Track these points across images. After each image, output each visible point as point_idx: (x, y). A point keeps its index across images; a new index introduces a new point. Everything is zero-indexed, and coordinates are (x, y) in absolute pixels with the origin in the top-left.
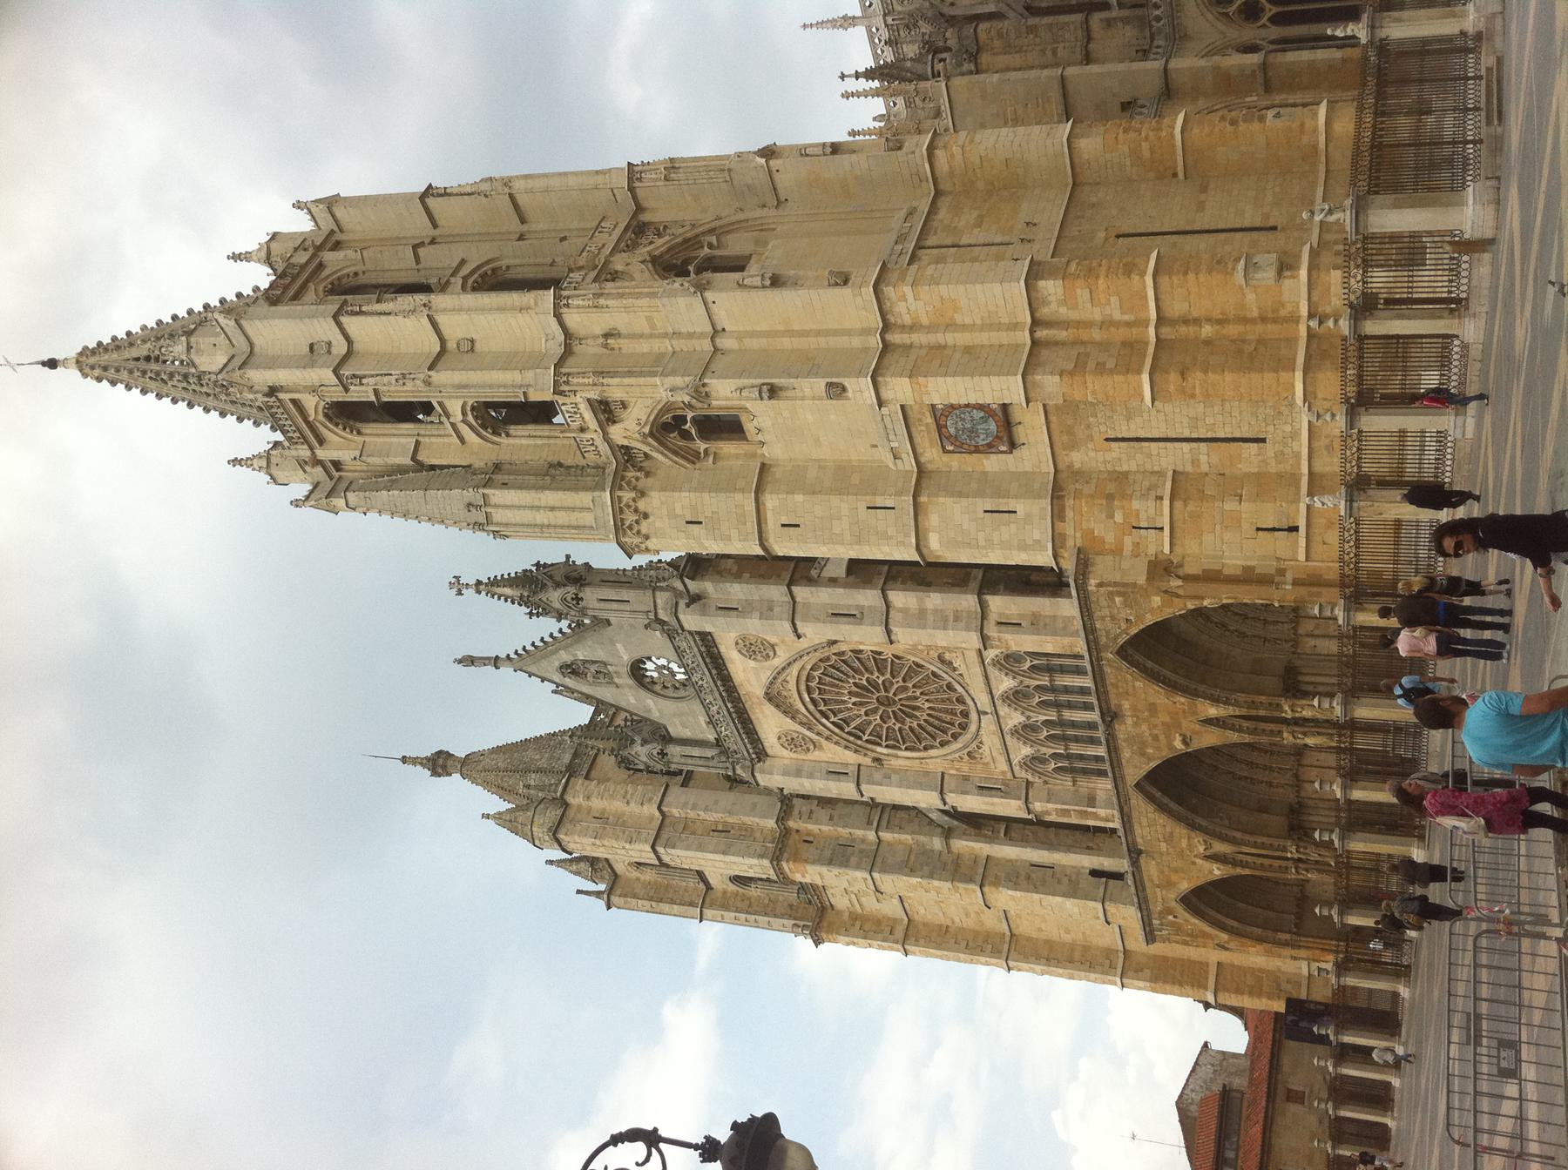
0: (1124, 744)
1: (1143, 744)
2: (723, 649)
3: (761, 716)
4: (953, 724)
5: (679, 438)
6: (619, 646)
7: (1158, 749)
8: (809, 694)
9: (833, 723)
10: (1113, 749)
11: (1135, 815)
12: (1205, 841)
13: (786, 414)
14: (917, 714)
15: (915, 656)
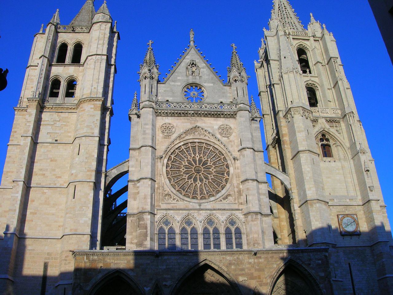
0: (235, 257)
1: (238, 264)
2: (221, 119)
3: (183, 121)
4: (186, 192)
5: (321, 138)
6: (212, 85)
7: (235, 270)
8: (198, 142)
9: (180, 146)
10: (233, 253)
11: (184, 257)
12: (170, 286)
13: (337, 171)
14: (192, 179)
15: (231, 186)
